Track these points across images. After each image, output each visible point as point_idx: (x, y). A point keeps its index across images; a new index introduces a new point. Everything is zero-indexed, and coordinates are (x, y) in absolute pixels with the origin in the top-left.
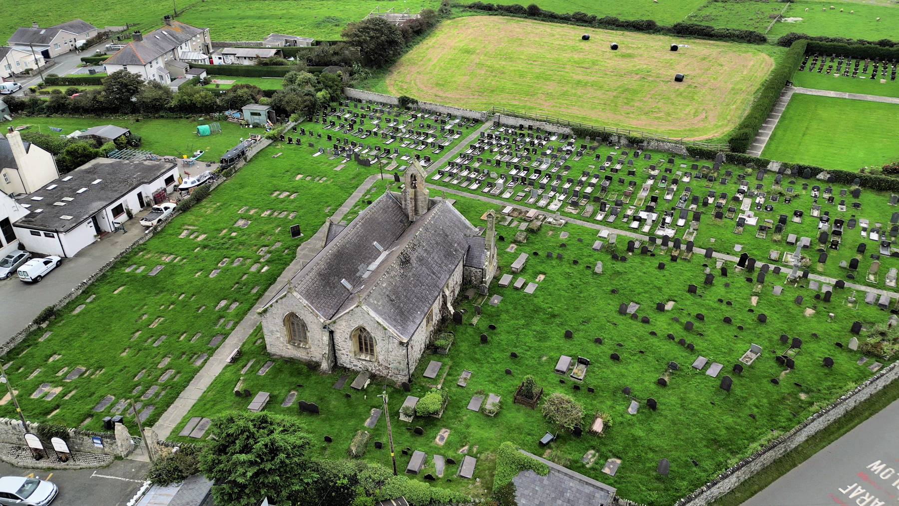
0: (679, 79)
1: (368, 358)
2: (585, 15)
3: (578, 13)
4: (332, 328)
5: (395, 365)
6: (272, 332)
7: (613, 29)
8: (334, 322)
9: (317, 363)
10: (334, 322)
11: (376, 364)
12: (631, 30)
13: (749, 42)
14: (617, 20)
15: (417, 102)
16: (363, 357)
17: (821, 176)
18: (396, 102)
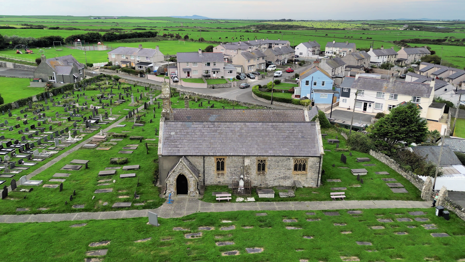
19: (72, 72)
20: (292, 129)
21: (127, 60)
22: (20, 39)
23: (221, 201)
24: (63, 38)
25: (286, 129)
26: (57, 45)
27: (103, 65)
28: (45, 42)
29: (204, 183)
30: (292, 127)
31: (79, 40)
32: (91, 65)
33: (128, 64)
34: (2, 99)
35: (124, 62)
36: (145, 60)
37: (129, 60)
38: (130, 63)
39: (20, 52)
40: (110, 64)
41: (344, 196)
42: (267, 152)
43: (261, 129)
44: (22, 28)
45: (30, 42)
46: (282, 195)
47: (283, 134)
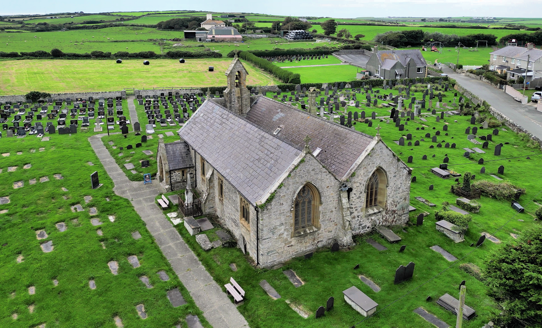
0: (211, 70)
1: (376, 211)
2: (103, 53)
3: (96, 52)
4: (349, 185)
5: (402, 203)
6: (273, 231)
7: (128, 59)
8: (353, 175)
9: (331, 242)
10: (353, 175)
11: (384, 213)
12: (140, 59)
13: (215, 57)
14: (128, 53)
15: (49, 95)
16: (371, 211)
17: (347, 86)
18: (24, 100)
19: (394, 67)
20: (273, 151)
21: (506, 65)
22: (441, 36)
23: (159, 205)
24: (496, 38)
25: (268, 147)
26: (482, 45)
27: (474, 67)
28: (468, 40)
29: (196, 186)
30: (275, 146)
31: (514, 40)
32: (461, 67)
33: (505, 70)
34: (300, 81)
35: (502, 67)
36: (524, 66)
37: (509, 65)
38: (509, 69)
39: (425, 49)
40: (485, 67)
41: (238, 298)
42: (225, 169)
43: (250, 136)
44: (494, 28)
45: (452, 40)
46: (201, 238)
47: (260, 153)
